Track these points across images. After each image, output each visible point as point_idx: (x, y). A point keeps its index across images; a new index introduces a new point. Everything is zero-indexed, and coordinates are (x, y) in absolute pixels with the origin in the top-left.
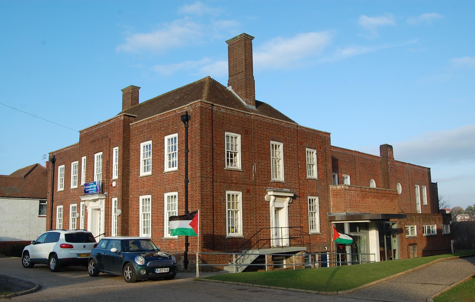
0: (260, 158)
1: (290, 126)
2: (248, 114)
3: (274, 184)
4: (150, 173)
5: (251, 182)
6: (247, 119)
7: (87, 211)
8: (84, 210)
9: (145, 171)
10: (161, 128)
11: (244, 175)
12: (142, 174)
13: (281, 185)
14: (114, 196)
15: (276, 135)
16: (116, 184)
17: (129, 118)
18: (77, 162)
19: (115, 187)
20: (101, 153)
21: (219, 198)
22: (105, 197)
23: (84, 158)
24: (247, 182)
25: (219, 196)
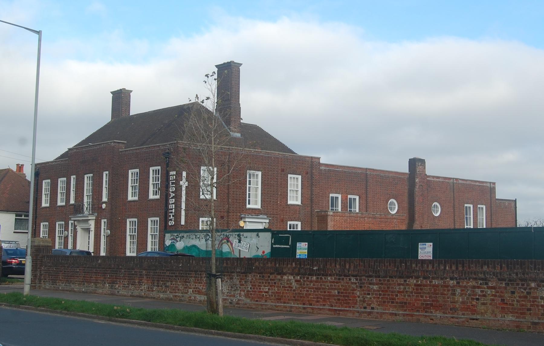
0: (235, 187)
1: (270, 155)
2: (225, 148)
3: (250, 211)
4: (136, 198)
5: (225, 210)
6: (224, 153)
7: (77, 230)
8: (73, 229)
9: (132, 197)
10: (147, 159)
11: (218, 204)
12: (130, 198)
13: (257, 211)
14: (104, 218)
15: (254, 165)
16: (106, 207)
17: (119, 144)
18: (65, 179)
19: (104, 209)
20: (92, 175)
21: (193, 224)
22: (95, 218)
23: (73, 177)
24: (221, 210)
25: (194, 222)
